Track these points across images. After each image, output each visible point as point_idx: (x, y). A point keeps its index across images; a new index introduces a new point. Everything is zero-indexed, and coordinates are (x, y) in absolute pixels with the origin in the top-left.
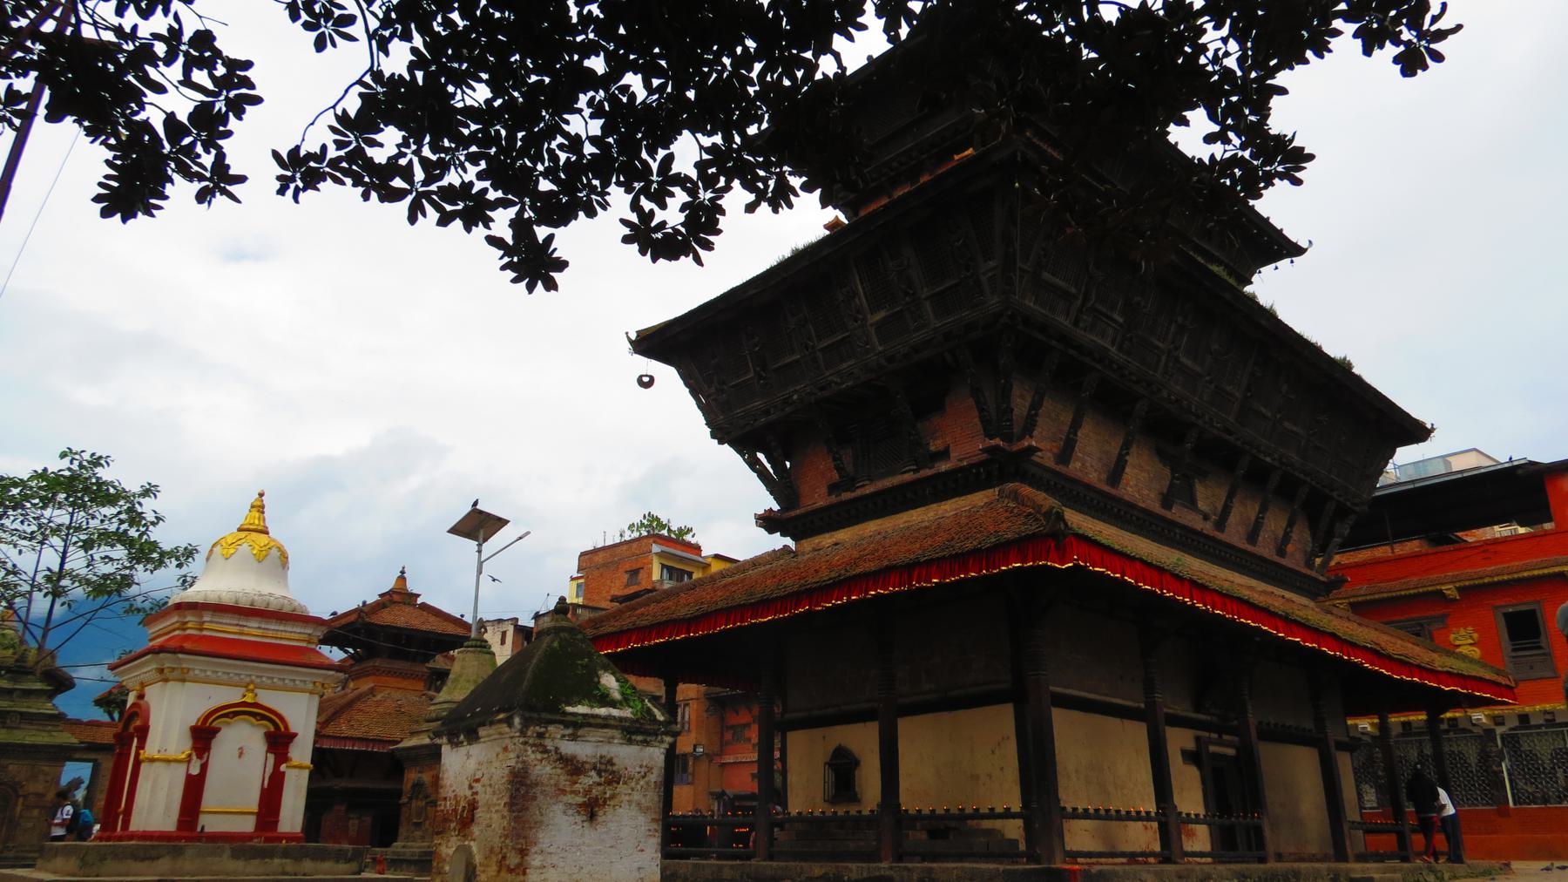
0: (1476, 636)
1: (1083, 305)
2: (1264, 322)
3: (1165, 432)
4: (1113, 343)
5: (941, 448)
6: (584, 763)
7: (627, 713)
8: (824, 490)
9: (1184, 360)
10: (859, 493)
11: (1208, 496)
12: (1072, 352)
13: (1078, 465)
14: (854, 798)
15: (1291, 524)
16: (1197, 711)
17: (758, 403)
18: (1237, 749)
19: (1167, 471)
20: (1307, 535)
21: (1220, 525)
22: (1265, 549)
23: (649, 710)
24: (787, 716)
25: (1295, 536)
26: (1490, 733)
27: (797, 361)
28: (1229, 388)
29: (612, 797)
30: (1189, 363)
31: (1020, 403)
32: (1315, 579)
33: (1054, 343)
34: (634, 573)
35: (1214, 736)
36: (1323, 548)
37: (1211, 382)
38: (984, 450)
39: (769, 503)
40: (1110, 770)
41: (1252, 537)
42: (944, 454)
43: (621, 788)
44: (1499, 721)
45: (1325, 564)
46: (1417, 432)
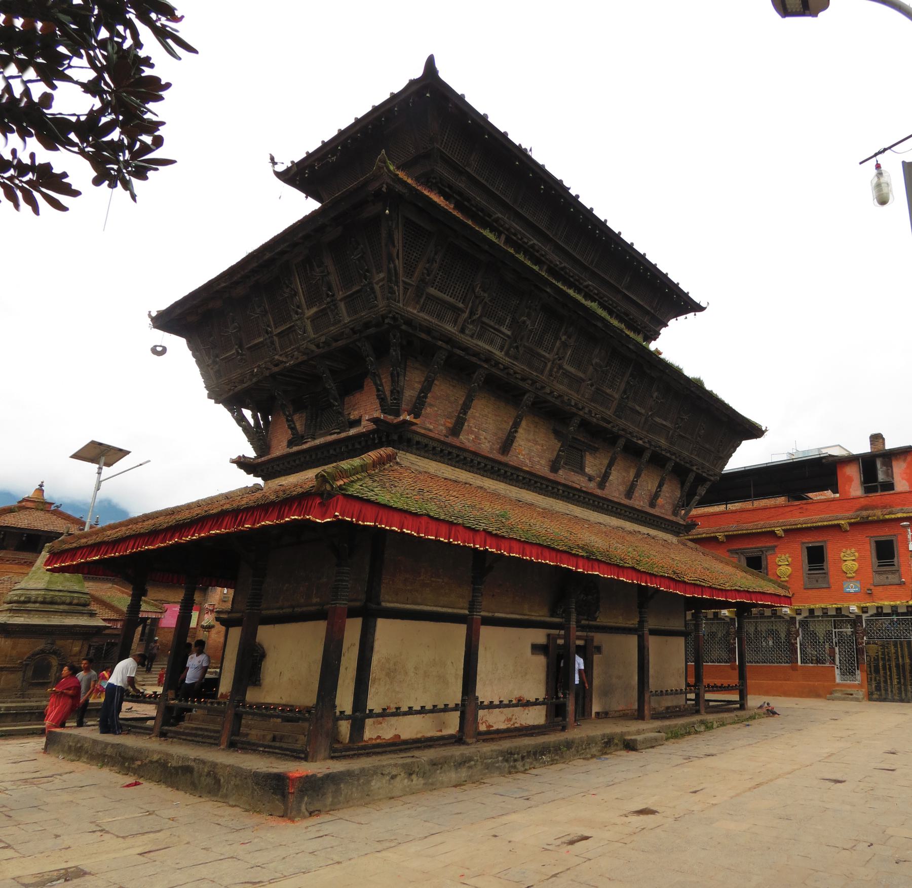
0: (790, 560)
9: (566, 366)
11: (593, 465)
13: (472, 437)
21: (602, 485)
22: (639, 501)
28: (608, 391)
32: (678, 524)
37: (592, 385)
41: (629, 494)
44: (798, 612)
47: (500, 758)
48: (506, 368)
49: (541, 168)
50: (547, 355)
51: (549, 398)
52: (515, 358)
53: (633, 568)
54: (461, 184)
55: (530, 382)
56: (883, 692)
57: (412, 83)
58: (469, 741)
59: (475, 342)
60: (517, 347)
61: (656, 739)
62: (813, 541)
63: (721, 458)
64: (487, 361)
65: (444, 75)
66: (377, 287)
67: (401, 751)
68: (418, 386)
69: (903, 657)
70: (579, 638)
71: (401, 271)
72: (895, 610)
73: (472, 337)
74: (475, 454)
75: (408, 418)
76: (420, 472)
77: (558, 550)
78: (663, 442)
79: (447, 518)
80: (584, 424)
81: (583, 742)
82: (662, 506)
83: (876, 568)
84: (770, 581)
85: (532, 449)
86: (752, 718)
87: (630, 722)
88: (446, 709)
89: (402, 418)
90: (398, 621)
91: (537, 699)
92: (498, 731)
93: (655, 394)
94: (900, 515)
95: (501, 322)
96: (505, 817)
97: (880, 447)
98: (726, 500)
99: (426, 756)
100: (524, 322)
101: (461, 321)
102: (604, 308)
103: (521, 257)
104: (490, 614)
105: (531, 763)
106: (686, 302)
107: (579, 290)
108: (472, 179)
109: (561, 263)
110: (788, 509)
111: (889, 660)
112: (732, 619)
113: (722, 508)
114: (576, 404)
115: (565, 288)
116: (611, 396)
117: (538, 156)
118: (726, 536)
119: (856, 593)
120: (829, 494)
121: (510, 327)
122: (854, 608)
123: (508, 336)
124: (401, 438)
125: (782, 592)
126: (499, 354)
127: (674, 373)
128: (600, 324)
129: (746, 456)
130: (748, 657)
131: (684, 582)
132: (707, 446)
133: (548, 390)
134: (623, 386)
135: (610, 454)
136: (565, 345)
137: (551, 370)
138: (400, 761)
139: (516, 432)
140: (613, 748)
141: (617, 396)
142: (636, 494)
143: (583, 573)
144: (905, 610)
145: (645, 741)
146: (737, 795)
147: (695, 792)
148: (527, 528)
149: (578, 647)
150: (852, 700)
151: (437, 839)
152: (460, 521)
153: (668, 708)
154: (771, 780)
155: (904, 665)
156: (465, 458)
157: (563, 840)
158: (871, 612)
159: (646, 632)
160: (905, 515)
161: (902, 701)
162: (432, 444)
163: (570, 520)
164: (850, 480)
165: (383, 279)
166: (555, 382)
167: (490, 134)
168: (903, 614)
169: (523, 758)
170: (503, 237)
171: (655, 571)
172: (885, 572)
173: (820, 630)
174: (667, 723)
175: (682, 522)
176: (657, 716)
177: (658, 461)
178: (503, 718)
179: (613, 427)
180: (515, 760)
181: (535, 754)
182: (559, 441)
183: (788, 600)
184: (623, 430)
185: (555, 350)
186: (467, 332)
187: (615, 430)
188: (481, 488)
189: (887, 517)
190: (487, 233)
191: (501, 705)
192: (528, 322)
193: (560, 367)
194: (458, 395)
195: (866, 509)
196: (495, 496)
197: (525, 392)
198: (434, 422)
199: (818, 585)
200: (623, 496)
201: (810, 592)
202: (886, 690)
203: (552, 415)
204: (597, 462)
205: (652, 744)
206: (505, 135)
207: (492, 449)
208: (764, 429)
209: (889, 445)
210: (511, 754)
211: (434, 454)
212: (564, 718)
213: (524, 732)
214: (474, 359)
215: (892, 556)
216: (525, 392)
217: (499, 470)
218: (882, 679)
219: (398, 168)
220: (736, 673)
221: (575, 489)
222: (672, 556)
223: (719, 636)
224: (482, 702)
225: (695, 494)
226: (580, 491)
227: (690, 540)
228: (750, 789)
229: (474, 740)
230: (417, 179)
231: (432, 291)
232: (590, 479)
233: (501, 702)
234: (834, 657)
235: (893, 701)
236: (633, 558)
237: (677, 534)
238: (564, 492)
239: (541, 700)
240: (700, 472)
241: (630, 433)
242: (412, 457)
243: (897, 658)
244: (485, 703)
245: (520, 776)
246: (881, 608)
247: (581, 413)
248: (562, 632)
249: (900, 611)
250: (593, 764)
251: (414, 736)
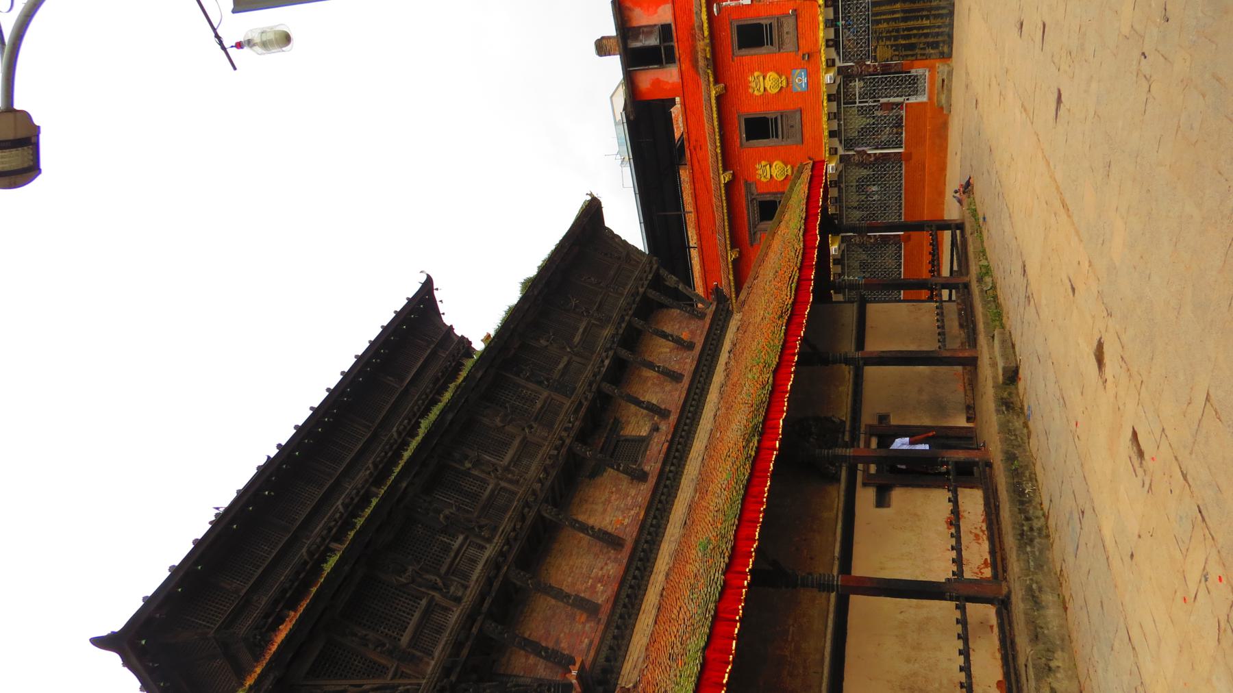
1: (440, 590)
2: (479, 375)
11: (637, 425)
12: (486, 605)
13: (600, 587)
16: (839, 480)
18: (871, 435)
21: (664, 414)
22: (686, 363)
26: (843, 159)
28: (539, 405)
30: (510, 453)
33: (474, 630)
37: (531, 427)
41: (676, 377)
44: (834, 151)
45: (703, 302)
46: (592, 212)
47: (1029, 549)
48: (508, 542)
49: (242, 494)
50: (490, 487)
51: (548, 483)
52: (495, 529)
53: (775, 372)
54: (264, 601)
55: (526, 510)
56: (940, 38)
57: (127, 663)
58: (1005, 591)
59: (472, 584)
60: (481, 527)
61: (1003, 342)
62: (739, 132)
63: (628, 254)
64: (498, 567)
65: (116, 622)
67: (1018, 681)
68: (532, 659)
69: (894, 12)
70: (868, 444)
71: (379, 682)
72: (830, 23)
73: (466, 587)
74: (622, 583)
75: (574, 673)
76: (647, 657)
77: (751, 474)
78: (607, 332)
79: (708, 623)
80: (583, 436)
81: (1007, 439)
82: (693, 333)
83: (774, 49)
84: (792, 189)
85: (614, 506)
86: (974, 213)
87: (981, 377)
88: (963, 622)
89: (574, 681)
90: (845, 684)
91: (950, 500)
92: (992, 552)
93: (543, 342)
94: (704, 17)
95: (446, 548)
96: (1107, 543)
97: (613, 43)
98: (684, 247)
99: (1025, 648)
100: (447, 517)
101: (445, 603)
102: (427, 410)
103: (360, 522)
104: (837, 562)
105: (1035, 508)
106: (420, 302)
107: (405, 444)
108: (255, 588)
109: (368, 468)
110: (696, 164)
111: (897, 31)
112: (843, 240)
113: (695, 255)
114: (556, 449)
115: (402, 463)
116: (545, 402)
117: (225, 498)
118: (732, 248)
119: (808, 75)
120: (676, 111)
121: (454, 537)
122: (828, 77)
123: (466, 539)
125: (807, 174)
126: (489, 551)
127: (516, 320)
128: (450, 417)
129: (625, 222)
130: (893, 219)
131: (794, 304)
132: (612, 273)
133: (537, 486)
134: (531, 386)
135: (623, 403)
136: (477, 463)
137: (510, 481)
138: (1032, 683)
139: (592, 528)
140: (1015, 399)
141: (545, 394)
142: (676, 368)
143: (781, 441)
144: (831, 10)
145: (1005, 356)
146: (1077, 233)
147: (1073, 290)
148: (720, 516)
149: (879, 445)
150: (950, 80)
151: (1135, 633)
152: (712, 606)
153: (961, 326)
154: (1058, 188)
155: (904, 11)
156: (628, 596)
157: (1137, 464)
158: (833, 55)
159: (859, 354)
160: (704, 9)
161: (951, 14)
162: (609, 641)
163: (711, 457)
164: (657, 83)
166: (527, 476)
167: (196, 563)
168: (836, 12)
169: (1028, 519)
170: (334, 545)
171: (778, 345)
172: (780, 36)
173: (858, 122)
174: (981, 326)
175: (713, 307)
176: (972, 340)
177: (632, 339)
178: (974, 546)
179: (586, 398)
180: (1031, 529)
181: (1022, 503)
182: (605, 470)
183: (818, 166)
184: (590, 385)
185: (483, 476)
186: (460, 594)
187: (590, 396)
188: (667, 575)
189: (706, 33)
190: (328, 567)
191: (957, 548)
192: (447, 512)
193: (506, 469)
194: (544, 606)
195: (697, 61)
196: (679, 557)
198: (580, 638)
199: (798, 126)
200: (679, 386)
201: (807, 136)
202: (938, 34)
203: (570, 478)
204: (633, 420)
205: (1009, 346)
206: (198, 543)
207: (616, 560)
208: (589, 198)
209: (610, 30)
210: (1022, 535)
211: (623, 639)
212: (976, 464)
213: (993, 517)
214: (496, 585)
215: (759, 26)
217: (644, 551)
218: (923, 40)
219: (242, 685)
220: (914, 234)
221: (669, 448)
222: (759, 319)
223: (865, 257)
224: (954, 573)
225: (676, 289)
226: (671, 442)
227: (737, 296)
228: (1069, 216)
229: (1004, 584)
230: (257, 659)
231: (405, 640)
232: (656, 429)
233: (953, 548)
234: (893, 104)
235: (951, 25)
236: (761, 372)
237: (729, 314)
238: (673, 464)
239: (950, 495)
240: (646, 283)
241: (595, 376)
242: (627, 667)
243: (895, 20)
244: (955, 569)
245: (1052, 522)
246: (827, 41)
247: (568, 441)
248: (860, 466)
249: (831, 16)
250: (1036, 425)
251: (999, 663)
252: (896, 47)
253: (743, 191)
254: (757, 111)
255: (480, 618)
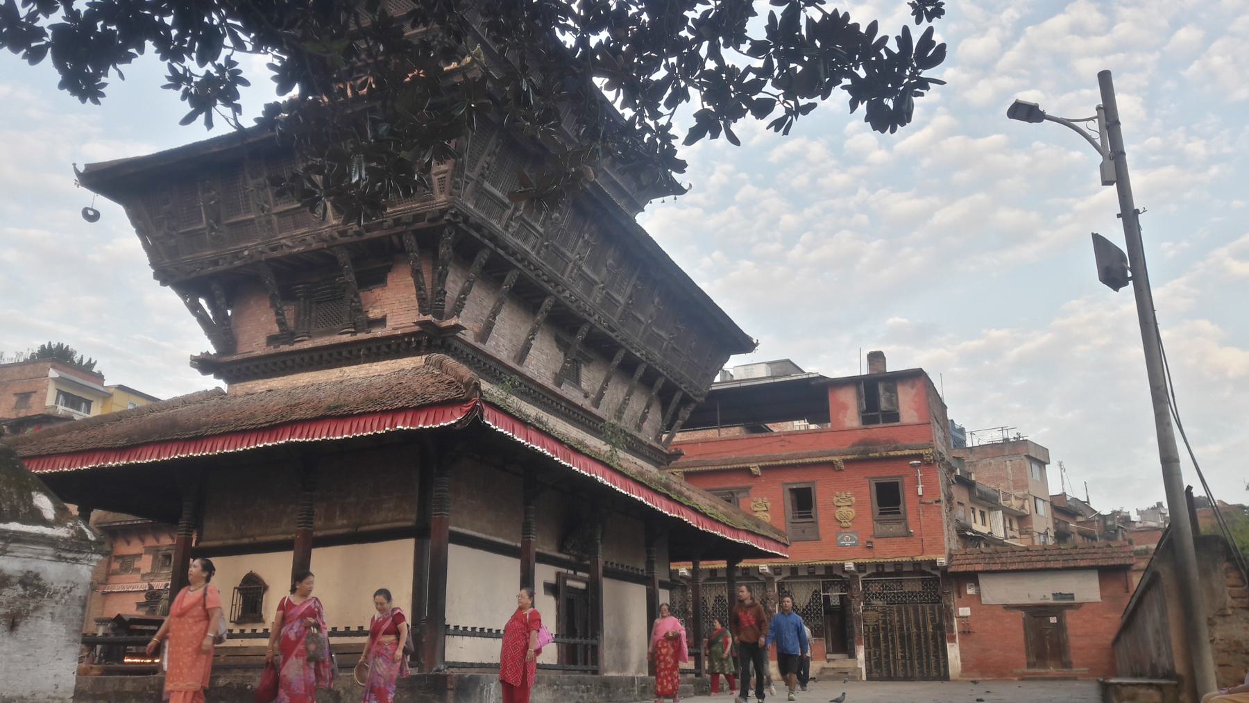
3: (564, 324)
4: (533, 248)
5: (379, 316)
6: (10, 576)
7: (61, 532)
8: (263, 340)
10: (297, 346)
11: (591, 377)
14: (259, 619)
15: (648, 407)
16: (560, 551)
17: (208, 253)
19: (562, 355)
20: (659, 416)
21: (596, 403)
22: (627, 423)
23: (82, 531)
24: (201, 544)
25: (649, 416)
26: (769, 579)
27: (252, 220)
29: (36, 608)
31: (453, 285)
34: (24, 397)
35: (571, 572)
36: (669, 427)
38: (417, 324)
39: (206, 346)
40: (487, 594)
42: (382, 322)
43: (46, 601)
45: (669, 439)
48: (536, 269)
52: (545, 259)
62: (798, 480)
64: (521, 261)
66: (435, 179)
78: (658, 356)
93: (657, 300)
95: (537, 220)
121: (543, 225)
124: (443, 342)
134: (628, 291)
141: (622, 301)
165: (446, 172)
187: (618, 340)
193: (580, 268)
197: (546, 294)
214: (512, 259)
216: (546, 294)
252: (876, 630)
253: (741, 485)
254: (820, 498)
255: (492, 246)
